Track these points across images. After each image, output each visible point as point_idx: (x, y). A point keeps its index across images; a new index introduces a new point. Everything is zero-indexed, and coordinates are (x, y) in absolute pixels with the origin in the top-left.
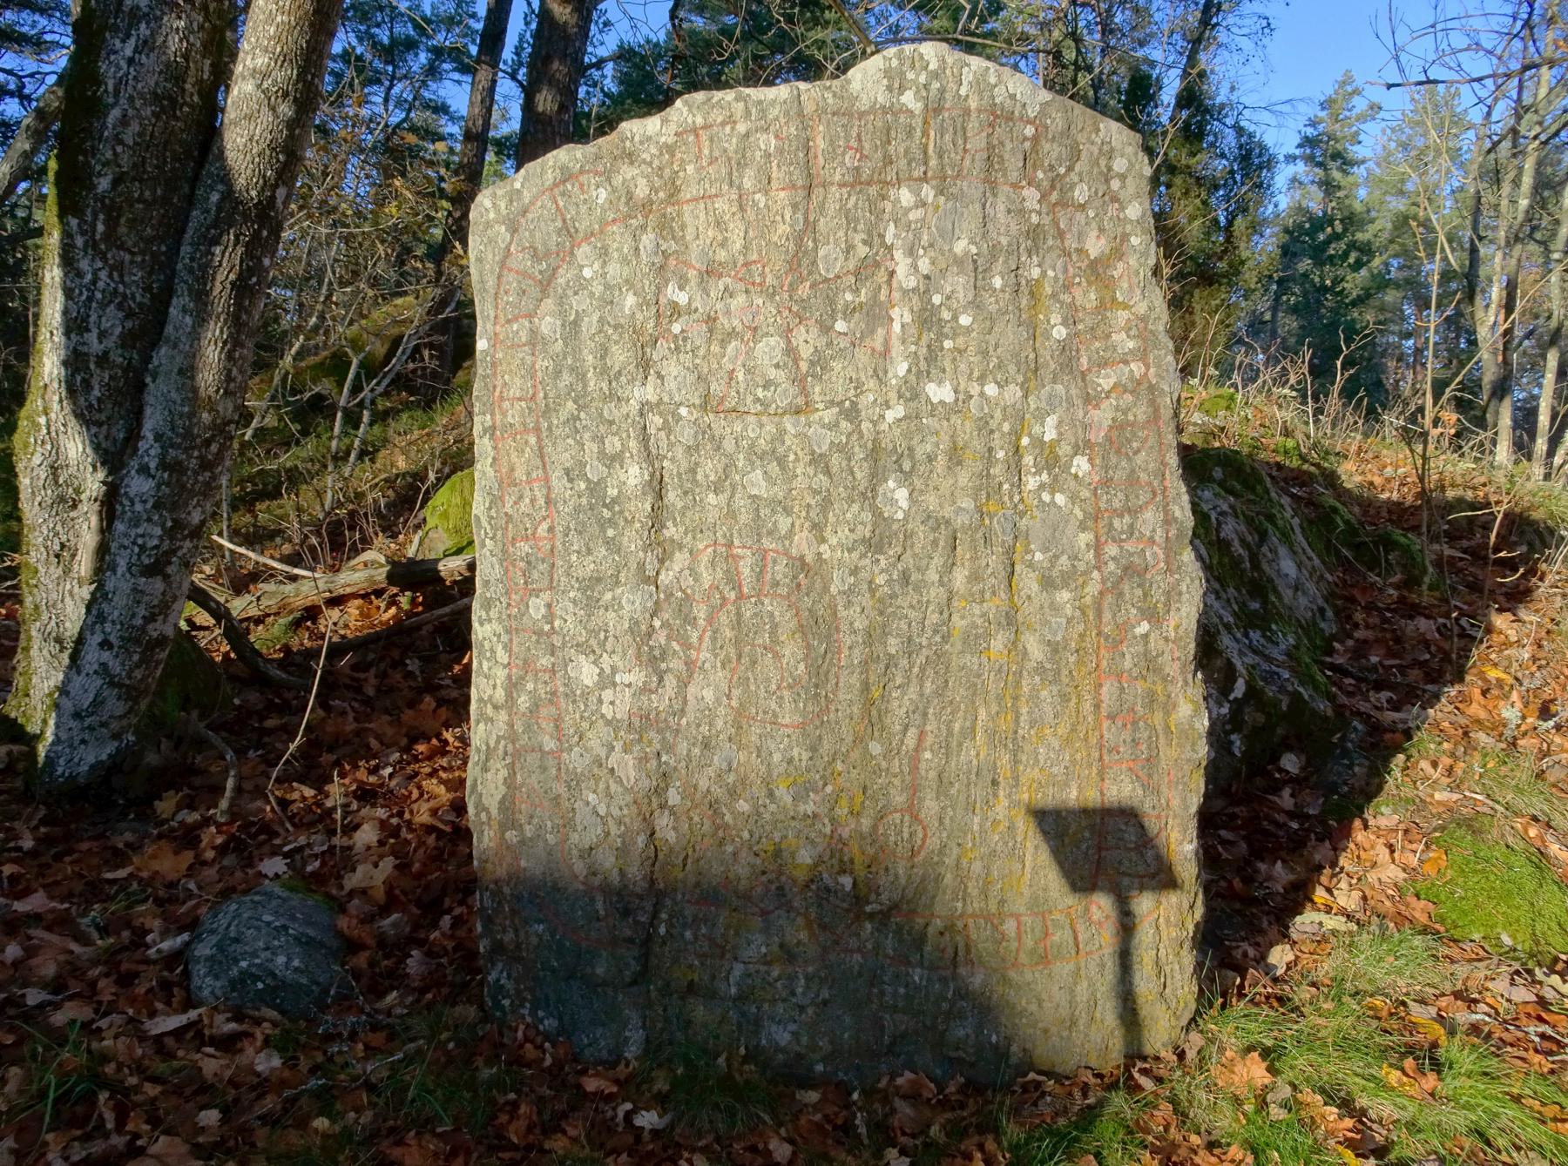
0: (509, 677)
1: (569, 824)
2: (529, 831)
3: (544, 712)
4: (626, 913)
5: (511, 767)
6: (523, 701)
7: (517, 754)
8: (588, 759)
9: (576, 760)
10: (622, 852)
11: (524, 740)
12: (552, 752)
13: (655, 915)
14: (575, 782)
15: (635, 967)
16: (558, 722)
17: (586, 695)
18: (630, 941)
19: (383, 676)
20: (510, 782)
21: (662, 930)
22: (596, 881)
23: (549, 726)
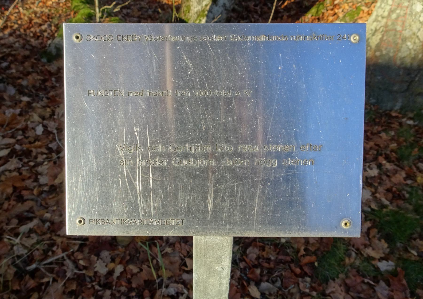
0: (391, 9)
1: (399, 51)
2: (384, 52)
3: (400, 19)
4: (409, 74)
5: (383, 36)
6: (394, 16)
7: (386, 31)
8: (411, 33)
9: (407, 33)
10: (413, 59)
11: (390, 27)
12: (399, 31)
13: (416, 76)
14: (404, 40)
15: (405, 87)
16: (404, 22)
17: (417, 13)
18: (407, 81)
19: (261, 8)
20: (381, 39)
21: (417, 79)
22: (402, 66)
23: (400, 23)
